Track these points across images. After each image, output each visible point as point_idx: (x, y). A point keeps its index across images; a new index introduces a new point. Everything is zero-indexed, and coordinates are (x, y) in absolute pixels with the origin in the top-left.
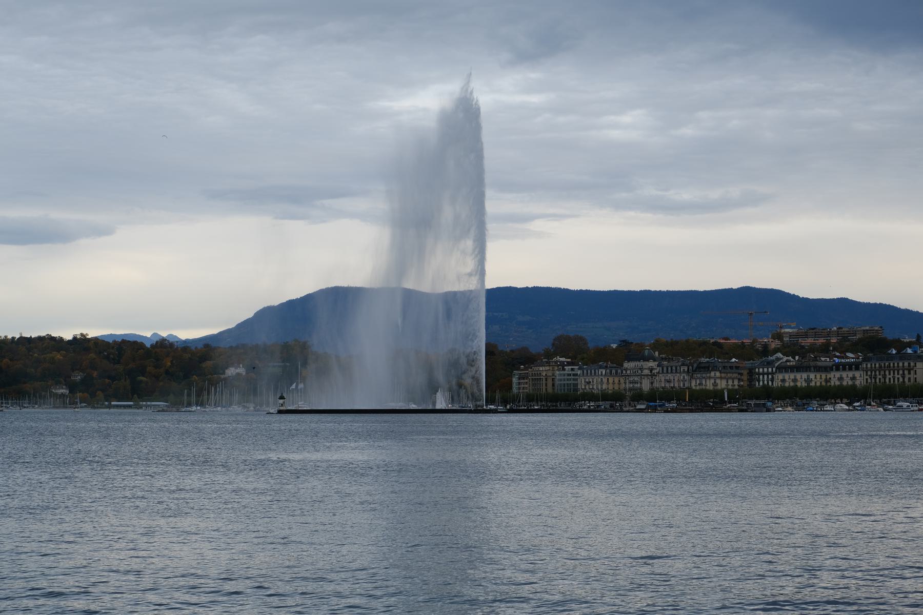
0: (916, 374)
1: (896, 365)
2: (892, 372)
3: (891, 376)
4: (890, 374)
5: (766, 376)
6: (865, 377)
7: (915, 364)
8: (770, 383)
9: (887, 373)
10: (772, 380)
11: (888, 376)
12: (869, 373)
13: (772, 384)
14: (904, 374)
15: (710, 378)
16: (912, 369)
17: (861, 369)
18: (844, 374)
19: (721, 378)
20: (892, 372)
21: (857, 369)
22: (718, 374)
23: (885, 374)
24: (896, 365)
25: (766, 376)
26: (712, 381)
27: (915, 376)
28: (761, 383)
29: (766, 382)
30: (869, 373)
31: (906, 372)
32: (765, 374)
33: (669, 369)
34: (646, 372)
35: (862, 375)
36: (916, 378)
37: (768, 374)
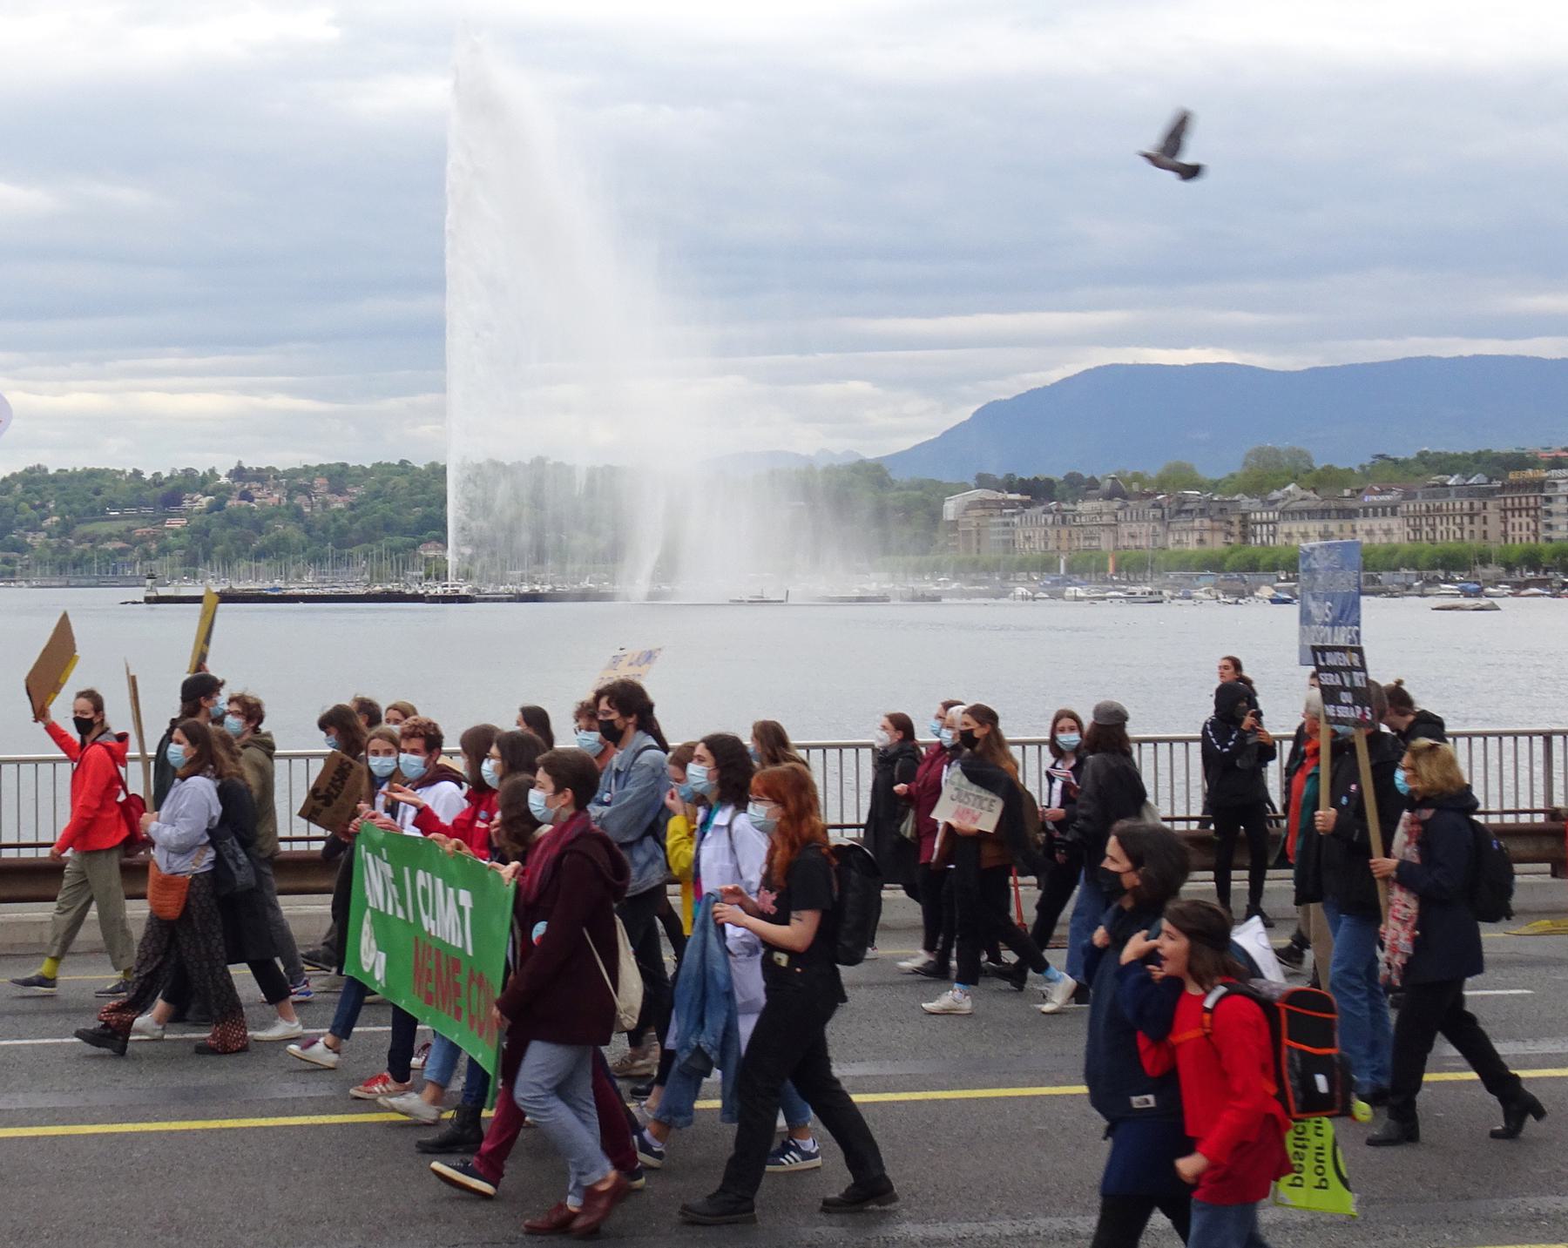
0: (1485, 523)
1: (1451, 507)
3: (1443, 528)
4: (1441, 524)
7: (1485, 504)
9: (1438, 520)
11: (1440, 528)
12: (1412, 522)
14: (1462, 523)
15: (1193, 530)
16: (1478, 514)
17: (1399, 514)
19: (1213, 530)
21: (1394, 513)
22: (1207, 523)
24: (1451, 507)
26: (1196, 536)
27: (1484, 527)
31: (1466, 520)
34: (1106, 519)
36: (1485, 532)
37: (1267, 523)
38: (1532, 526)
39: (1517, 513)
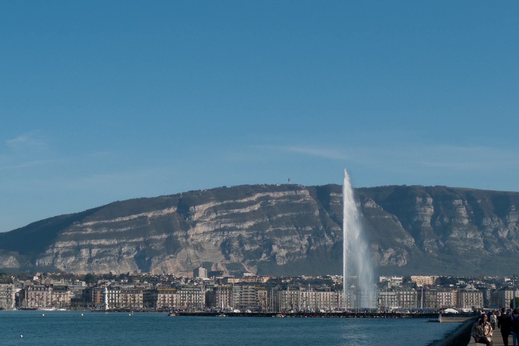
2: (195, 295)
4: (194, 296)
5: (114, 295)
6: (179, 297)
8: (117, 298)
10: (118, 297)
13: (118, 298)
18: (166, 295)
20: (195, 295)
23: (191, 295)
25: (114, 295)
28: (110, 298)
29: (114, 297)
30: (182, 295)
32: (114, 293)
33: (39, 289)
35: (177, 296)
38: (228, 297)
39: (222, 295)
